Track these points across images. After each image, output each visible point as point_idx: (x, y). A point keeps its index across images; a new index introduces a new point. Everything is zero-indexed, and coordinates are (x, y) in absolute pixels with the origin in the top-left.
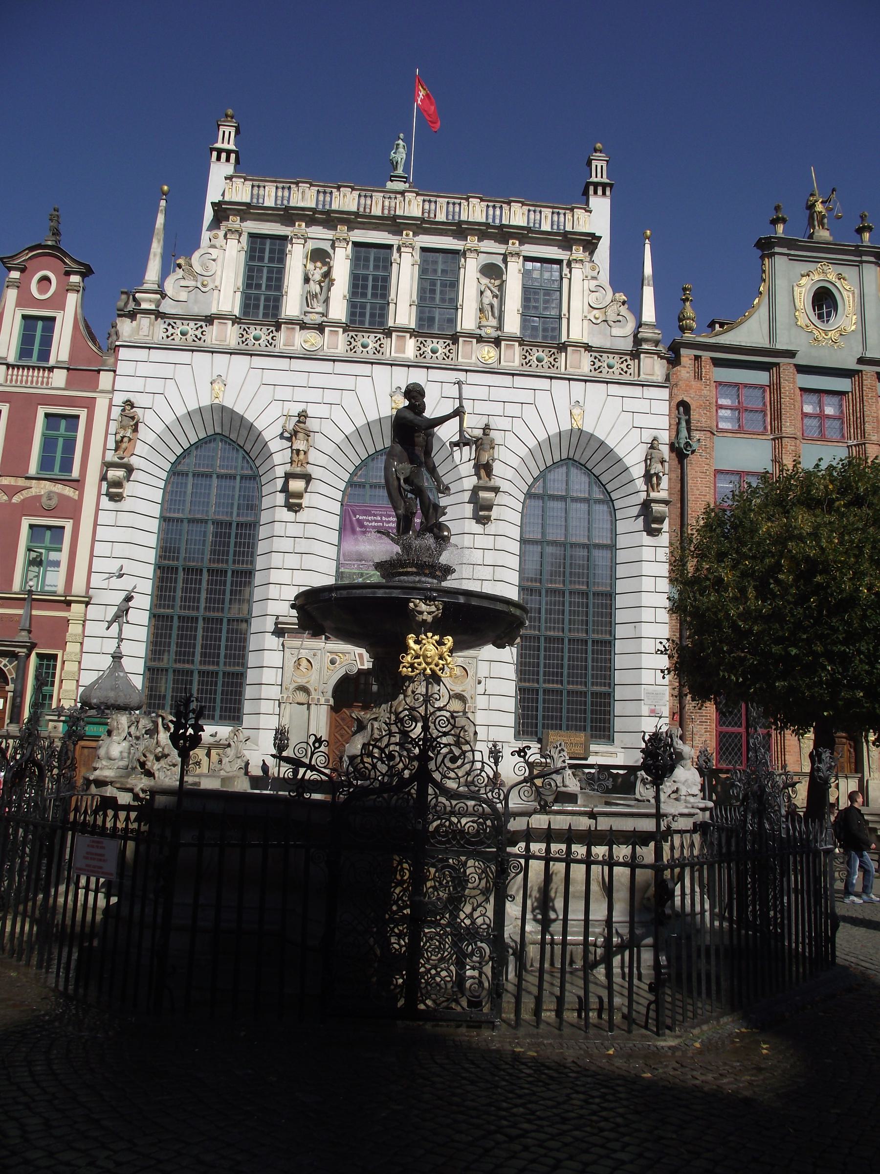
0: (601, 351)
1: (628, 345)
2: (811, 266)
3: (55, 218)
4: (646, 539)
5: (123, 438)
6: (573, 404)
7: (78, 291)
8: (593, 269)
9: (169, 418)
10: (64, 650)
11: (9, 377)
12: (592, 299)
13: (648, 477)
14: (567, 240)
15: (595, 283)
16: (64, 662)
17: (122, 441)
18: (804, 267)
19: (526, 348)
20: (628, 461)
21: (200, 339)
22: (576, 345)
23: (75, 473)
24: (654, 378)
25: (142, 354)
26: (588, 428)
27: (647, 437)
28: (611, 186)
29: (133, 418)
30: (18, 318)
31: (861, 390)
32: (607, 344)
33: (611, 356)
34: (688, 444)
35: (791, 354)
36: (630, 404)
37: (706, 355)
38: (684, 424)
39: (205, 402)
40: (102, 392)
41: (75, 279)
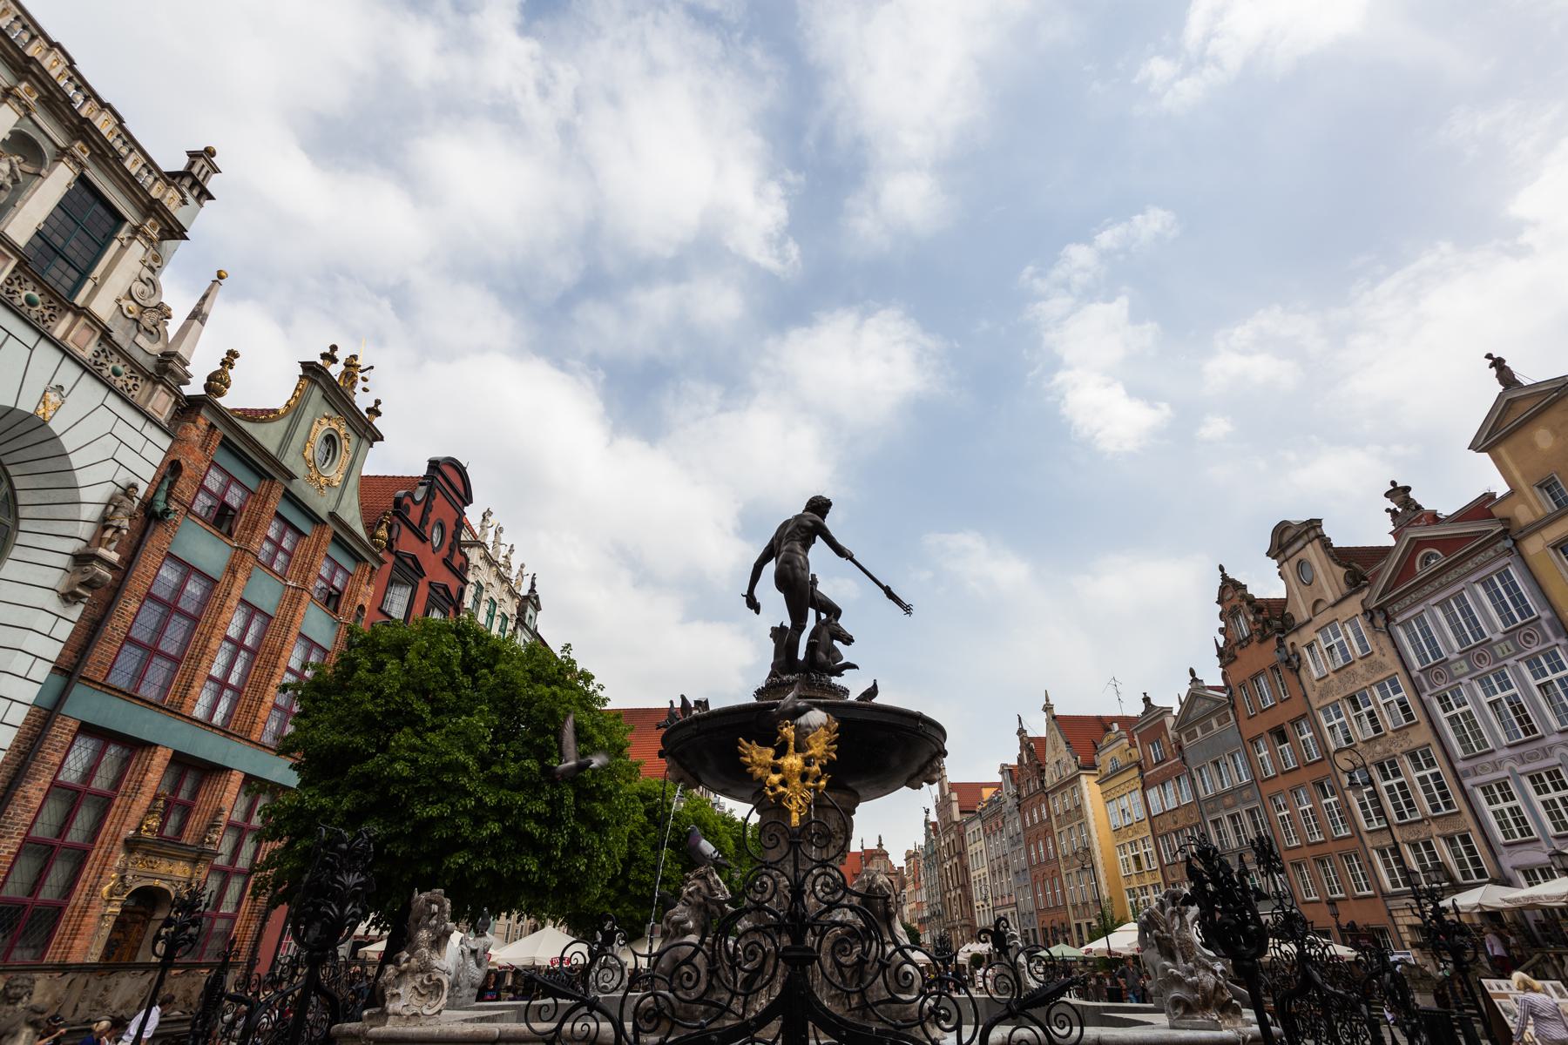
0: (116, 348)
1: (149, 364)
2: (333, 414)
4: (52, 602)
6: (53, 385)
8: (156, 259)
12: (138, 287)
13: (104, 523)
14: (152, 208)
15: (146, 274)
18: (328, 411)
19: (19, 273)
20: (85, 495)
22: (94, 321)
24: (162, 419)
26: (56, 426)
27: (123, 478)
28: (211, 197)
31: (319, 540)
32: (126, 347)
33: (122, 362)
34: (166, 512)
35: (291, 477)
36: (122, 430)
37: (221, 430)
38: (165, 487)
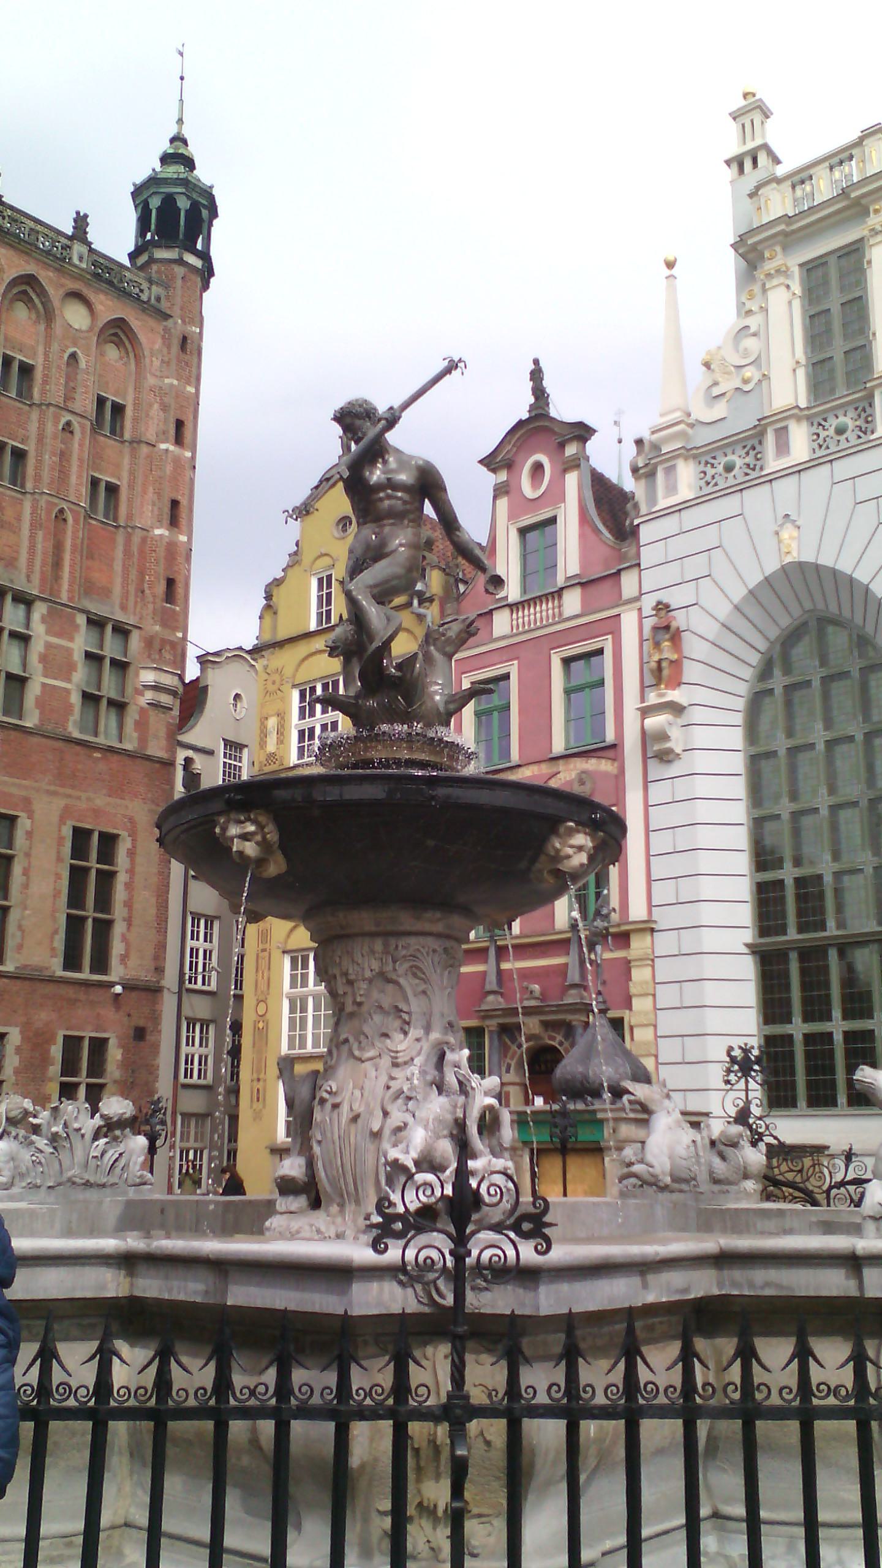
3: (537, 375)
5: (659, 662)
7: (578, 466)
9: (723, 610)
10: (630, 1007)
11: (515, 622)
16: (631, 1028)
17: (660, 669)
21: (754, 469)
23: (610, 737)
25: (668, 525)
29: (667, 628)
30: (514, 535)
39: (772, 566)
40: (630, 601)
41: (571, 450)
